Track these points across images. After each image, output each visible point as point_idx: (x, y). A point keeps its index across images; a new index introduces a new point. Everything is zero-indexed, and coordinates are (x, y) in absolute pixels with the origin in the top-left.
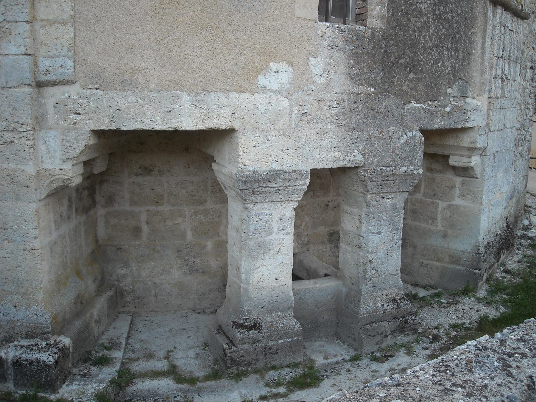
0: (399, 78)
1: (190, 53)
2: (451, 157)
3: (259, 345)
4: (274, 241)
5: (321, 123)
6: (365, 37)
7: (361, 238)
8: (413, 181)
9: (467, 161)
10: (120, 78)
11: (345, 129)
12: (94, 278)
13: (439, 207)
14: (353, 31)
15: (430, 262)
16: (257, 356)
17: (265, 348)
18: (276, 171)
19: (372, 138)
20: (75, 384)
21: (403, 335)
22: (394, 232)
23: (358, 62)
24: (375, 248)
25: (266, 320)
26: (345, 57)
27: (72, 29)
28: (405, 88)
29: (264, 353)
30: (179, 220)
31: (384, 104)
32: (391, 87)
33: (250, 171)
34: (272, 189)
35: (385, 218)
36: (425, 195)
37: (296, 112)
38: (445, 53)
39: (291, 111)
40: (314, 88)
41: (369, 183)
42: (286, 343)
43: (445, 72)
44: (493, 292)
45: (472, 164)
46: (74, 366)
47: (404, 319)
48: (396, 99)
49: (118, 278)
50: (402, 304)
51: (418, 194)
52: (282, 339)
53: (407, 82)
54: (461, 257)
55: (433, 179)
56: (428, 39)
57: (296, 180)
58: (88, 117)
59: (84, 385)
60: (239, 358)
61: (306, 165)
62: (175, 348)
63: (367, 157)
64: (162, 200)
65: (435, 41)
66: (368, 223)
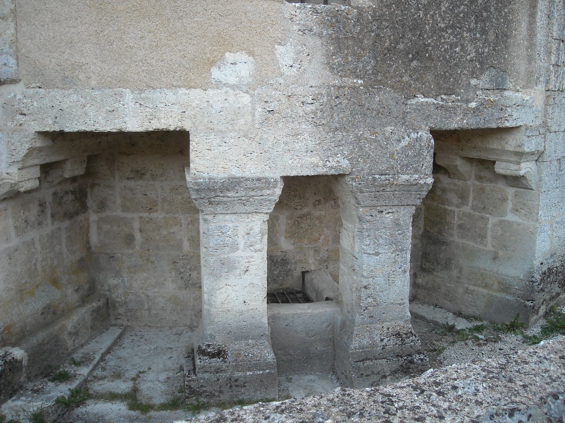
0: (397, 67)
1: (132, 45)
2: (497, 163)
3: (223, 375)
4: (241, 259)
5: (293, 122)
6: (349, 19)
7: (354, 258)
8: (419, 193)
9: (516, 169)
10: (61, 75)
11: (324, 129)
12: (77, 288)
13: (490, 222)
14: (331, 12)
15: (476, 288)
16: (220, 388)
17: (231, 380)
18: (236, 178)
19: (361, 140)
20: (21, 400)
21: (408, 377)
22: (397, 253)
23: (339, 49)
24: (372, 271)
25: (233, 347)
26: (322, 43)
27: (12, 25)
28: (406, 78)
29: (229, 384)
30: (175, 229)
31: (377, 98)
32: (387, 78)
33: (204, 178)
34: (233, 199)
35: (384, 236)
36: (474, 208)
37: (260, 110)
38: (465, 35)
39: (254, 109)
40: (282, 81)
41: (359, 194)
42: (255, 375)
43: (467, 59)
44: (548, 330)
45: (522, 173)
46: (29, 379)
47: (410, 358)
48: (394, 92)
49: (109, 288)
50: (407, 340)
51: (465, 206)
52: (250, 371)
53: (408, 72)
54: (512, 284)
55: (483, 190)
56: (439, 19)
57: (261, 189)
58: (32, 118)
59: (29, 402)
60: (198, 388)
61: (274, 172)
62: (149, 369)
63: (354, 163)
64: (155, 206)
65: (450, 20)
66: (362, 242)
